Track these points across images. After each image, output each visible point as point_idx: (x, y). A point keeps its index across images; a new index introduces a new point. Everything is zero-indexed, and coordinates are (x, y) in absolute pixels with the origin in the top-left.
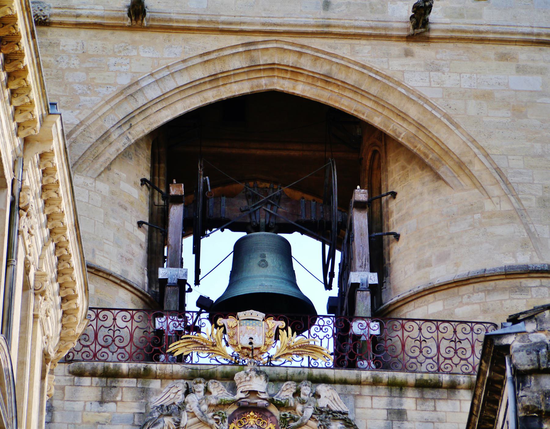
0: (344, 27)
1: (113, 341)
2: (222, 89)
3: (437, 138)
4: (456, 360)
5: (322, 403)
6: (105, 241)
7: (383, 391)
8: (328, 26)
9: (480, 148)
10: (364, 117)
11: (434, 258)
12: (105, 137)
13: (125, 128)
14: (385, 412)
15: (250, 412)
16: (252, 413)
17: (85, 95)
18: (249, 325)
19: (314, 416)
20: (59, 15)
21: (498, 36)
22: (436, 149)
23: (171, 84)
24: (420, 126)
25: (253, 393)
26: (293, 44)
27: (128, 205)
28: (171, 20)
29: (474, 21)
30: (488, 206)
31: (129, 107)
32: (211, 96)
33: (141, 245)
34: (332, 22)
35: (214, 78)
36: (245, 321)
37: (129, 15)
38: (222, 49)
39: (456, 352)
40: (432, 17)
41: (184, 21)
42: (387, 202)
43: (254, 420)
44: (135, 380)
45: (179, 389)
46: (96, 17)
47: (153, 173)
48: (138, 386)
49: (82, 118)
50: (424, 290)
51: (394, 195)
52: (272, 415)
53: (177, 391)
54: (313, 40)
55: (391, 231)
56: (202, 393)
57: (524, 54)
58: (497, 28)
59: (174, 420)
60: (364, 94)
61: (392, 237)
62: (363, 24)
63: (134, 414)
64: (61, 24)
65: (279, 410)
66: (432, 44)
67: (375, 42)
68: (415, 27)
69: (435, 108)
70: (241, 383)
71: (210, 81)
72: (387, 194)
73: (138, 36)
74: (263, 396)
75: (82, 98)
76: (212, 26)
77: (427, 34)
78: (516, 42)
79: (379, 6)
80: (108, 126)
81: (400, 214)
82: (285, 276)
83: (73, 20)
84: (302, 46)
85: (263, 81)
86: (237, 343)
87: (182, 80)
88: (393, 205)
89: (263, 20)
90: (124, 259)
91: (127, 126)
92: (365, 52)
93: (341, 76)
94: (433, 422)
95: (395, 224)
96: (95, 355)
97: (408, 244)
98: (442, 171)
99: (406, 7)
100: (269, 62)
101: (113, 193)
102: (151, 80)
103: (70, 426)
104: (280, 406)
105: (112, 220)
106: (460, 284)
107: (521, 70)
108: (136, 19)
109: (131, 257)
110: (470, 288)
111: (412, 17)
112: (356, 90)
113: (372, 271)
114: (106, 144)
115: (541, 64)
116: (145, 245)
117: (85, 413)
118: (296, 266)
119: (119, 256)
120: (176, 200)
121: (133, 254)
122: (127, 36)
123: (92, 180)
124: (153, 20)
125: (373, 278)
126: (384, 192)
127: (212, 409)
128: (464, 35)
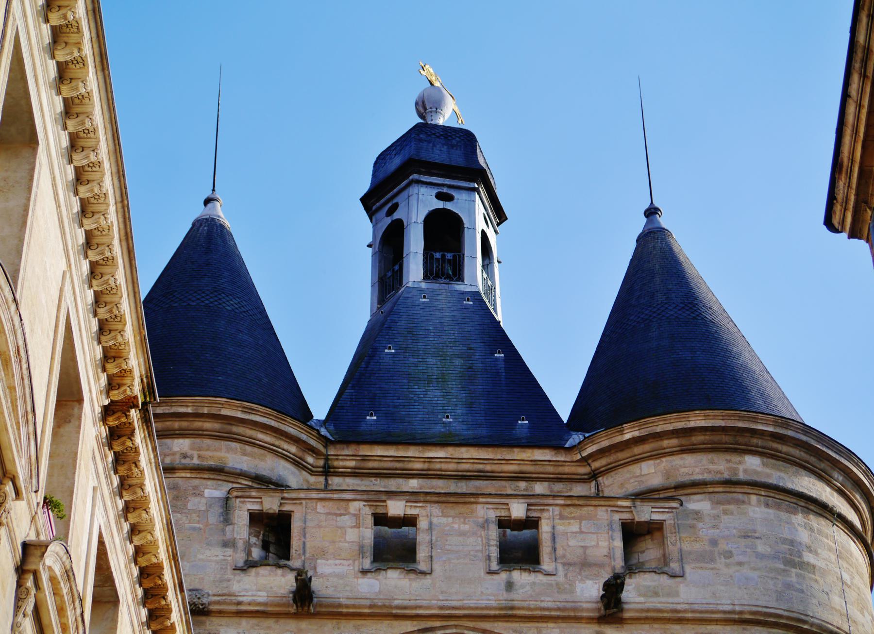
0: (529, 609)
8: (512, 608)
20: (218, 603)
21: (698, 615)
28: (340, 605)
29: (670, 600)
34: (516, 603)
37: (295, 601)
41: (354, 606)
46: (259, 604)
54: (496, 624)
58: (696, 607)
64: (221, 613)
66: (626, 627)
67: (564, 625)
68: (607, 606)
73: (304, 624)
76: (385, 611)
77: (620, 615)
78: (717, 621)
79: (567, 586)
83: (233, 608)
89: (440, 603)
99: (596, 586)
108: (302, 606)
111: (603, 597)
124: (321, 605)
128: (660, 615)
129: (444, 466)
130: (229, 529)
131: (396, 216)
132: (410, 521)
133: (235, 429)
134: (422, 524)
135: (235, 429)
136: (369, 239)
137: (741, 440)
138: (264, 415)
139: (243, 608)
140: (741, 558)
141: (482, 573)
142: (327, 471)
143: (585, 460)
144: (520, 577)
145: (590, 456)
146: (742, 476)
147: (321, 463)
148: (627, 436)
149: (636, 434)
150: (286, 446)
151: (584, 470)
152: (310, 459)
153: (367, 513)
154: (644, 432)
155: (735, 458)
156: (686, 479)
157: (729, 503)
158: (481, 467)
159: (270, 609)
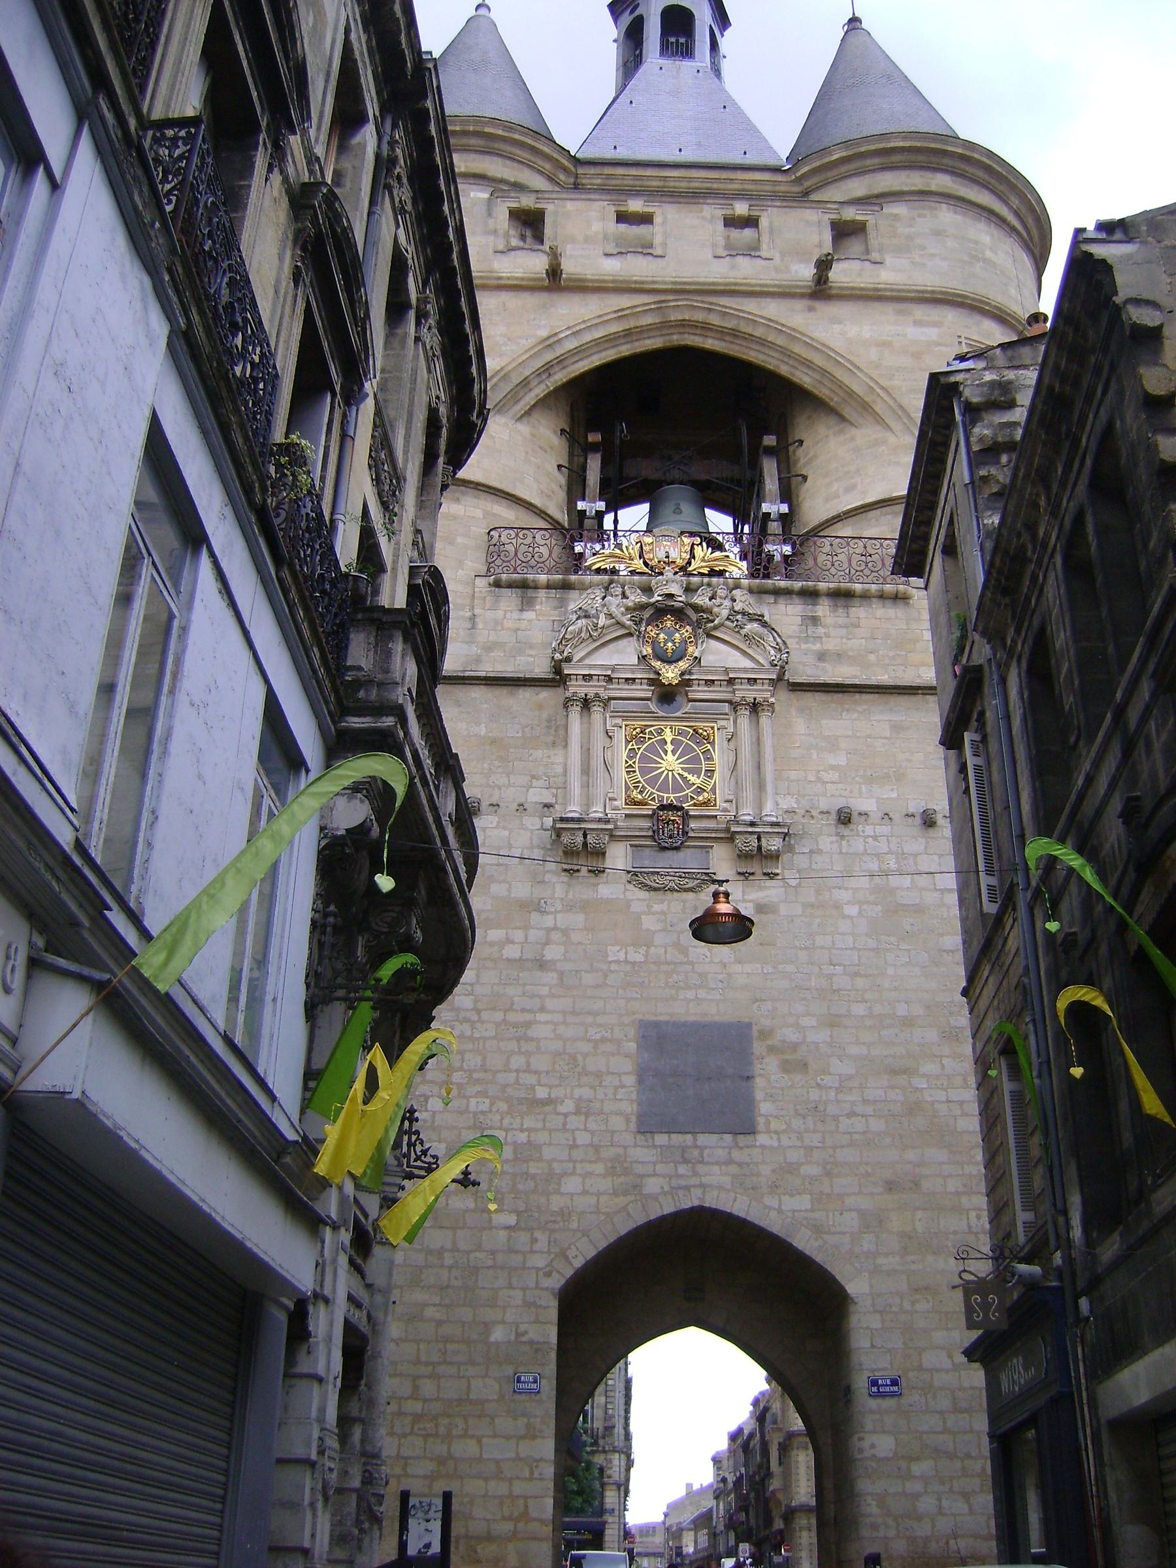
2: (637, 344)
4: (867, 572)
5: (738, 607)
7: (796, 599)
9: (883, 388)
10: (771, 367)
11: (841, 490)
12: (525, 384)
17: (505, 345)
21: (894, 294)
22: (841, 393)
23: (588, 337)
24: (824, 372)
25: (671, 596)
26: (703, 302)
28: (586, 280)
30: (892, 439)
31: (549, 356)
32: (625, 350)
35: (628, 334)
38: (635, 307)
40: (832, 275)
42: (794, 451)
46: (517, 278)
47: (572, 428)
50: (834, 518)
51: (801, 442)
57: (919, 311)
60: (772, 345)
62: (768, 282)
69: (838, 354)
71: (624, 336)
73: (555, 297)
74: (680, 599)
75: (503, 348)
82: (698, 521)
84: (711, 304)
85: (675, 337)
87: (598, 334)
92: (771, 309)
93: (749, 330)
95: (802, 467)
96: (515, 569)
98: (846, 411)
100: (680, 318)
101: (533, 435)
102: (568, 333)
104: (697, 608)
107: (917, 323)
110: (878, 512)
112: (762, 342)
114: (526, 390)
115: (937, 319)
120: (594, 448)
122: (544, 297)
124: (569, 279)
125: (784, 508)
126: (790, 441)
129: (677, 184)
130: (491, 222)
131: (637, 13)
132: (646, 219)
133: (496, 145)
134: (658, 220)
135: (496, 145)
136: (616, 36)
137: (933, 159)
138: (522, 134)
139: (503, 282)
140: (933, 251)
141: (710, 256)
142: (576, 187)
143: (799, 180)
144: (743, 262)
145: (803, 176)
146: (933, 188)
147: (572, 180)
148: (835, 157)
149: (844, 154)
150: (541, 163)
151: (796, 189)
152: (562, 177)
153: (611, 211)
154: (850, 153)
155: (928, 175)
156: (886, 190)
157: (923, 208)
158: (709, 185)
159: (524, 283)
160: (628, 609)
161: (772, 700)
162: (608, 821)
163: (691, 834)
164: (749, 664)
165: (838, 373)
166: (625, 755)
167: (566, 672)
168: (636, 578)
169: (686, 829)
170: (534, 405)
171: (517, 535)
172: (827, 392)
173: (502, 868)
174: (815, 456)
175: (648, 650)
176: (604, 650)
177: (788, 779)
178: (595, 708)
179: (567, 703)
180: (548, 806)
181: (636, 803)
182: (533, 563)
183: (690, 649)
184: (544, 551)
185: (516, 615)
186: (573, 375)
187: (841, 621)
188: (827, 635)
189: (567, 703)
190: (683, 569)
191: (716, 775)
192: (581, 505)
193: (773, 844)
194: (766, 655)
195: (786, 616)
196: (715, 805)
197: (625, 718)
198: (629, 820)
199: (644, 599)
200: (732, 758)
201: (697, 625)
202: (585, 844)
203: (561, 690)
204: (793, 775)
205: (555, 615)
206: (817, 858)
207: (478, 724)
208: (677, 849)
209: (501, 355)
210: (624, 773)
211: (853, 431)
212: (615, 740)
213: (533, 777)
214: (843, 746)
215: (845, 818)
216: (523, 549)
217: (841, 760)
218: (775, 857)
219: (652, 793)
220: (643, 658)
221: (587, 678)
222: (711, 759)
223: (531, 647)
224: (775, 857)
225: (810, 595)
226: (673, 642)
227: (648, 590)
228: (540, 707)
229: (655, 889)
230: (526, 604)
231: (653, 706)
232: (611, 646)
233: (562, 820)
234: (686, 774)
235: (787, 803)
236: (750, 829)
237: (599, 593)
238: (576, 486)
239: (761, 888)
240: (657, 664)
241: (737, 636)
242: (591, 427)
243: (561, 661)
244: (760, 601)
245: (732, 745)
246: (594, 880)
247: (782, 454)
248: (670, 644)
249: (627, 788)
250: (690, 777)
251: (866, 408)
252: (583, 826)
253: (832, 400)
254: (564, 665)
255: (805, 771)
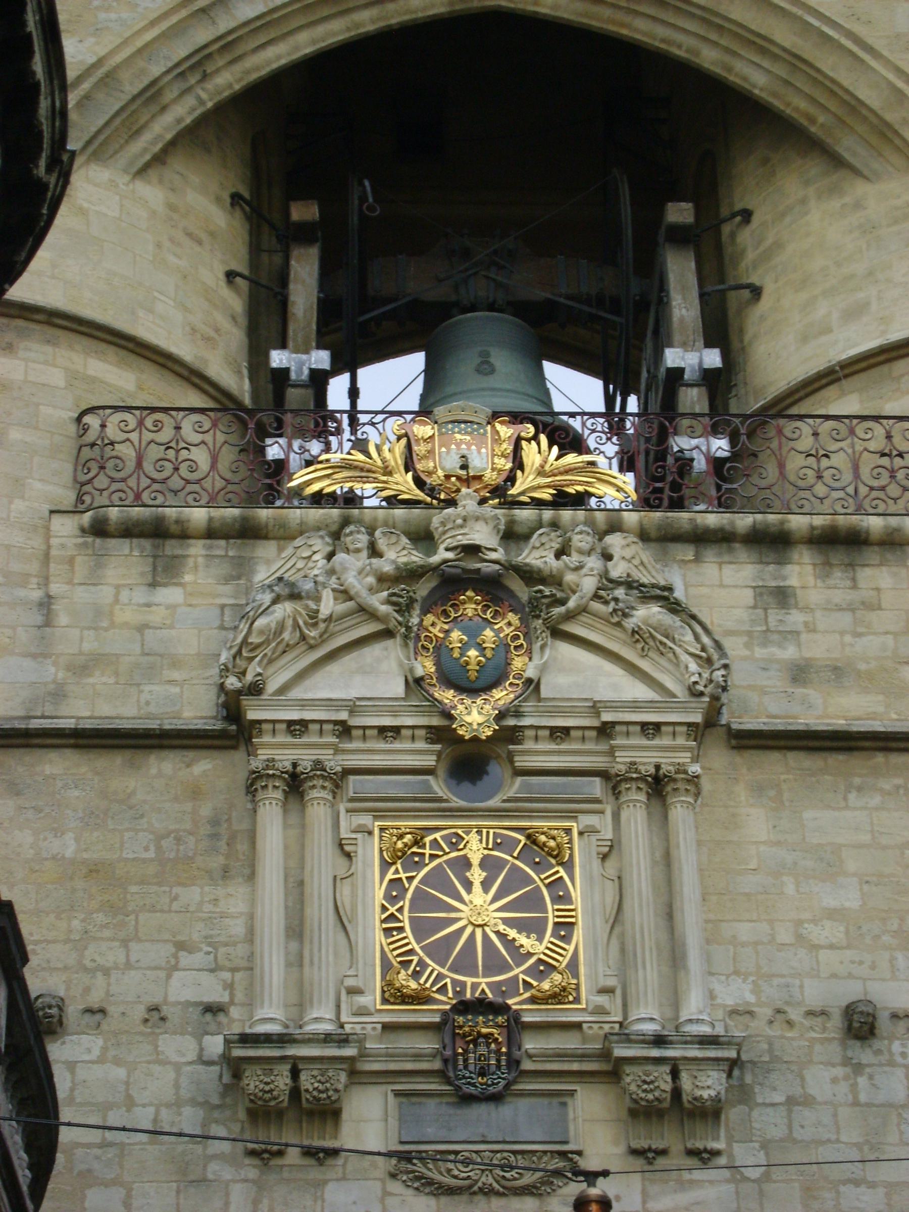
1: (176, 469)
3: (833, 81)
5: (618, 570)
6: (156, 294)
7: (742, 552)
12: (151, 95)
13: (192, 80)
14: (749, 593)
15: (466, 590)
16: (470, 593)
18: (459, 433)
19: (602, 593)
22: (832, 105)
24: (796, 61)
25: (473, 550)
27: (203, 236)
31: (202, 35)
33: (234, 318)
36: (450, 426)
39: (893, 477)
42: (733, 235)
43: (474, 606)
44: (222, 543)
45: (315, 549)
48: (231, 553)
49: (102, 53)
51: (747, 215)
52: (512, 594)
53: (309, 553)
55: (745, 281)
56: (365, 554)
59: (307, 607)
61: (746, 293)
63: (223, 607)
65: (527, 585)
70: (444, 533)
72: (734, 216)
74: (493, 556)
75: (102, 16)
80: (156, 70)
81: (762, 248)
82: (531, 391)
86: (435, 467)
88: (745, 236)
90: (199, 336)
91: (197, 76)
94: (853, 610)
96: (138, 496)
97: (778, 300)
101: (172, 207)
103: (86, 632)
104: (530, 576)
105: (172, 259)
106: (894, 354)
109: (212, 334)
113: (708, 344)
114: (154, 108)
116: (243, 321)
117: (118, 607)
118: (549, 385)
119: (188, 328)
120: (303, 234)
121: (217, 330)
123: (127, 178)
125: (713, 358)
126: (725, 212)
127: (386, 585)
160: (382, 579)
161: (695, 769)
162: (344, 1040)
163: (527, 1065)
164: (640, 692)
165: (828, 64)
166: (380, 893)
167: (252, 715)
168: (399, 513)
169: (516, 1054)
170: (172, 144)
171: (141, 423)
172: (803, 105)
173: (111, 1153)
174: (778, 245)
175: (425, 666)
176: (334, 668)
177: (733, 941)
178: (314, 794)
179: (254, 784)
180: (213, 1009)
181: (405, 998)
182: (176, 482)
183: (518, 663)
184: (201, 457)
185: (140, 595)
186: (254, 76)
187: (840, 596)
188: (811, 628)
189: (254, 784)
190: (498, 491)
191: (578, 935)
192: (278, 358)
193: (707, 1084)
194: (680, 672)
195: (722, 588)
196: (577, 1000)
197: (378, 814)
198: (392, 1036)
199: (416, 558)
200: (611, 897)
201: (531, 611)
202: (295, 1093)
203: (239, 756)
204: (744, 931)
205: (226, 594)
206: (805, 1115)
207: (58, 832)
208: (496, 1098)
209: (98, 32)
210: (379, 936)
211: (861, 188)
212: (359, 861)
213: (181, 946)
214: (851, 866)
215: (860, 1025)
216: (155, 452)
217: (849, 897)
218: (709, 1113)
219: (440, 977)
220: (415, 684)
221: (297, 727)
222: (565, 898)
223: (176, 663)
224: (709, 1113)
225: (772, 543)
226: (482, 649)
227: (423, 538)
228: (195, 793)
229: (451, 1191)
230: (164, 571)
231: (438, 787)
232: (349, 661)
233: (246, 1039)
234: (512, 933)
235: (735, 992)
236: (655, 1053)
237: (320, 545)
238: (266, 319)
239: (683, 1186)
240: (447, 696)
241: (617, 632)
242: (296, 190)
243: (239, 692)
244: (663, 559)
245: (611, 863)
246: (315, 1173)
247: (709, 244)
248: (473, 653)
249: (386, 965)
250: (522, 940)
251: (884, 133)
252: (292, 1051)
253: (813, 121)
254: (246, 701)
255: (771, 922)
